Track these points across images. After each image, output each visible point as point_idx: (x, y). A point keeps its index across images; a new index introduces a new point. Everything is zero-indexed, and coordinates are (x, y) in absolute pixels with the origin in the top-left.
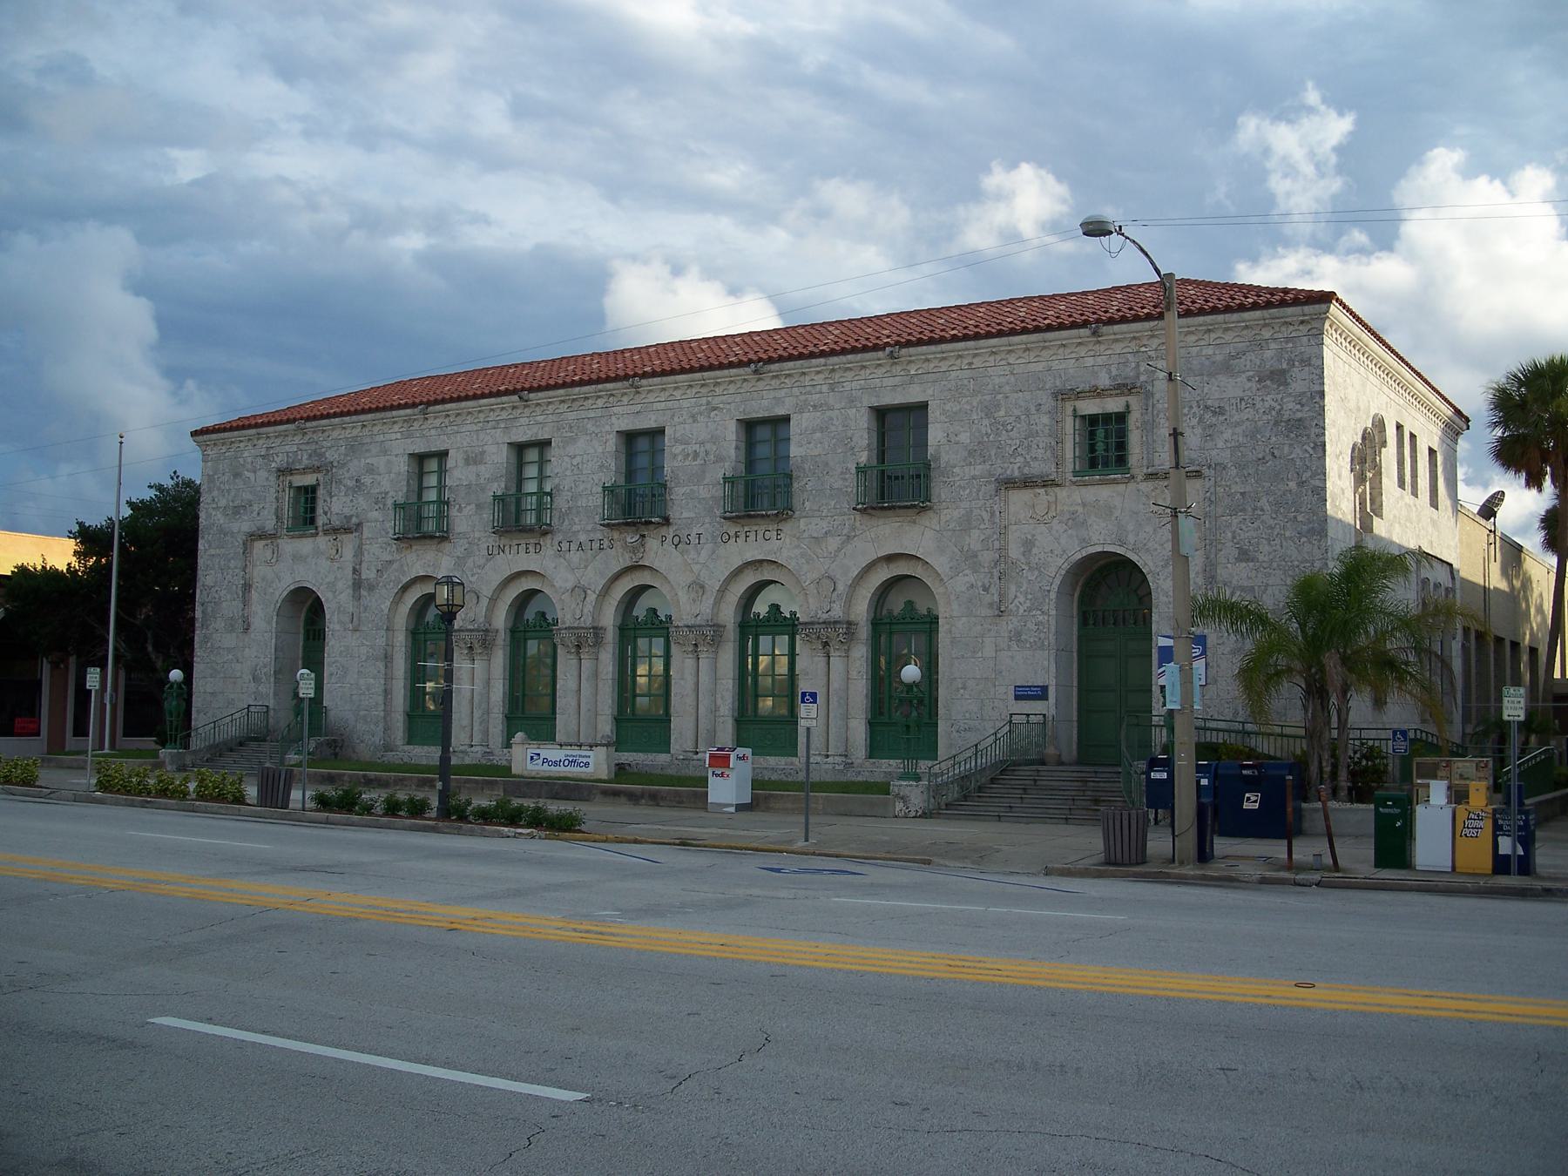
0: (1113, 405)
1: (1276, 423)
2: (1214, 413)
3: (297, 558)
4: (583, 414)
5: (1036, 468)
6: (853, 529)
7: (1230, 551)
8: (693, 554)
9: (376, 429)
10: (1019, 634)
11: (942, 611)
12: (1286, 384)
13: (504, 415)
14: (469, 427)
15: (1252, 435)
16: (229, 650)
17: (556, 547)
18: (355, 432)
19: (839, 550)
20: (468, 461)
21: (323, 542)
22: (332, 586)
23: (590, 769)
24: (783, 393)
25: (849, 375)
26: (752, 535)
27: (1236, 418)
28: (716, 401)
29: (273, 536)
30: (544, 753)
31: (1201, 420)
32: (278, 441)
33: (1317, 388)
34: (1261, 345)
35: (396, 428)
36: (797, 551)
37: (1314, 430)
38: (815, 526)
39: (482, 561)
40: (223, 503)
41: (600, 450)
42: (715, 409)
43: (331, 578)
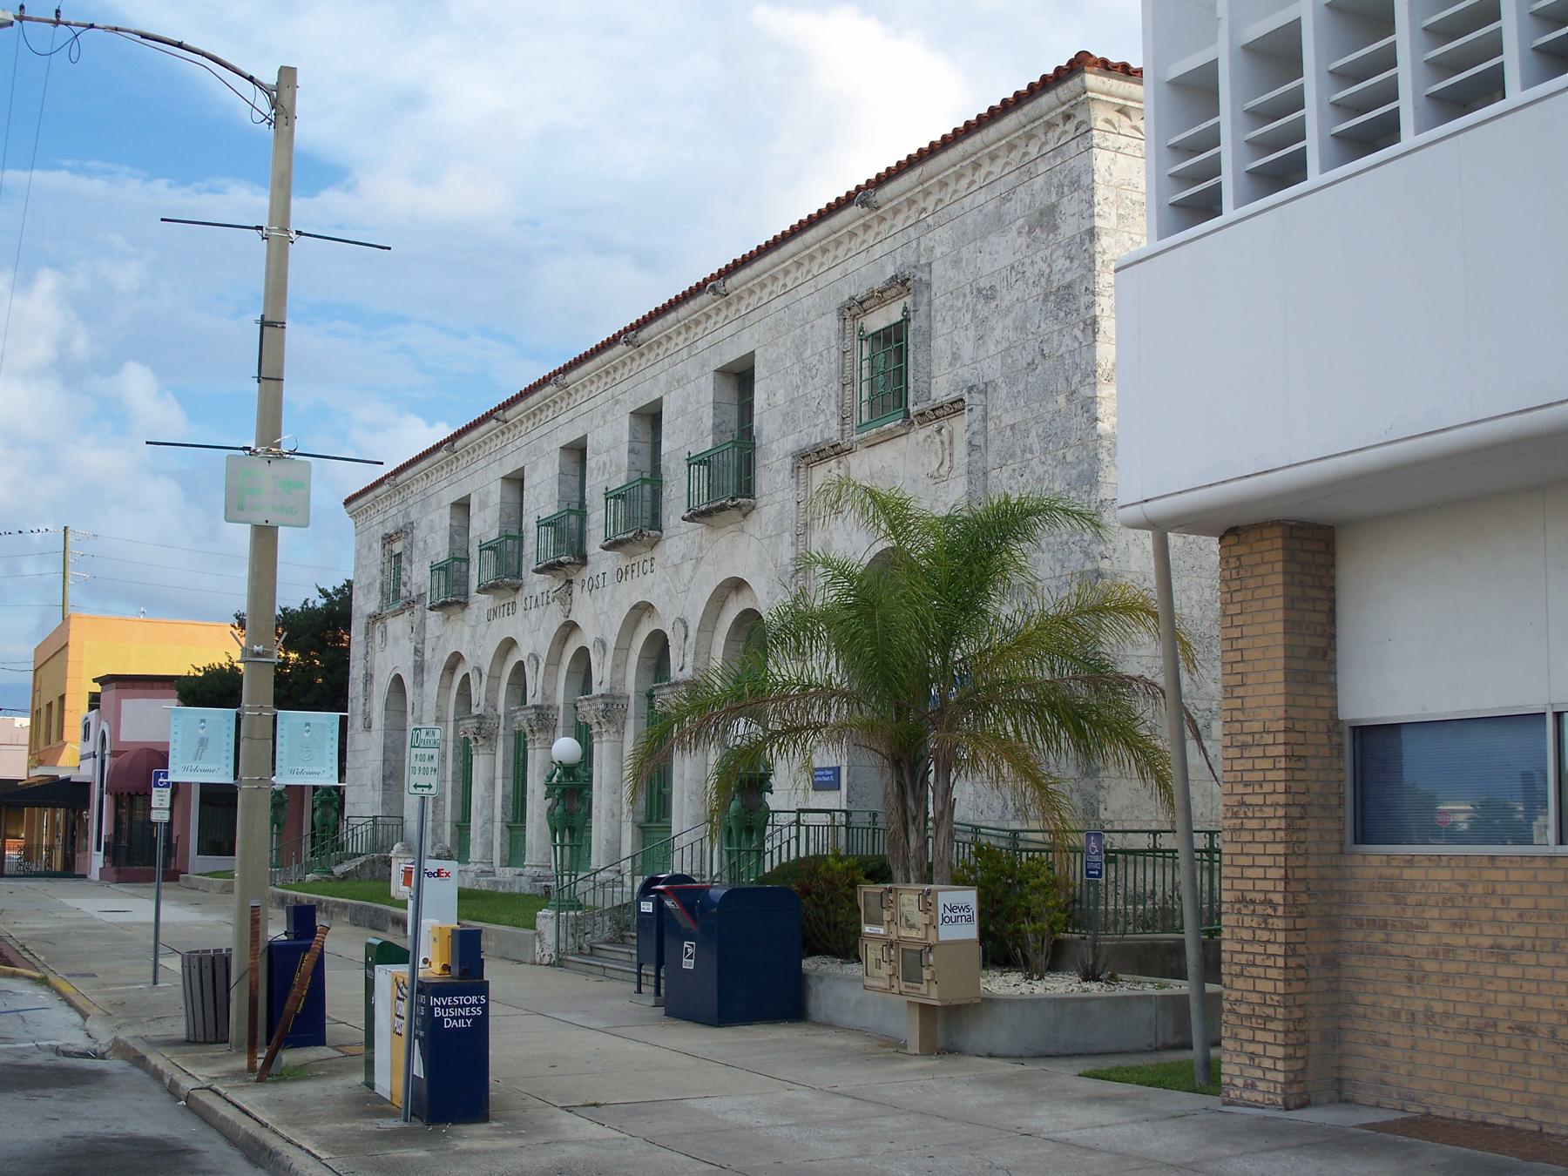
0: (893, 313)
2: (986, 297)
15: (1021, 328)
31: (974, 317)
33: (1087, 226)
37: (1084, 300)
42: (617, 402)
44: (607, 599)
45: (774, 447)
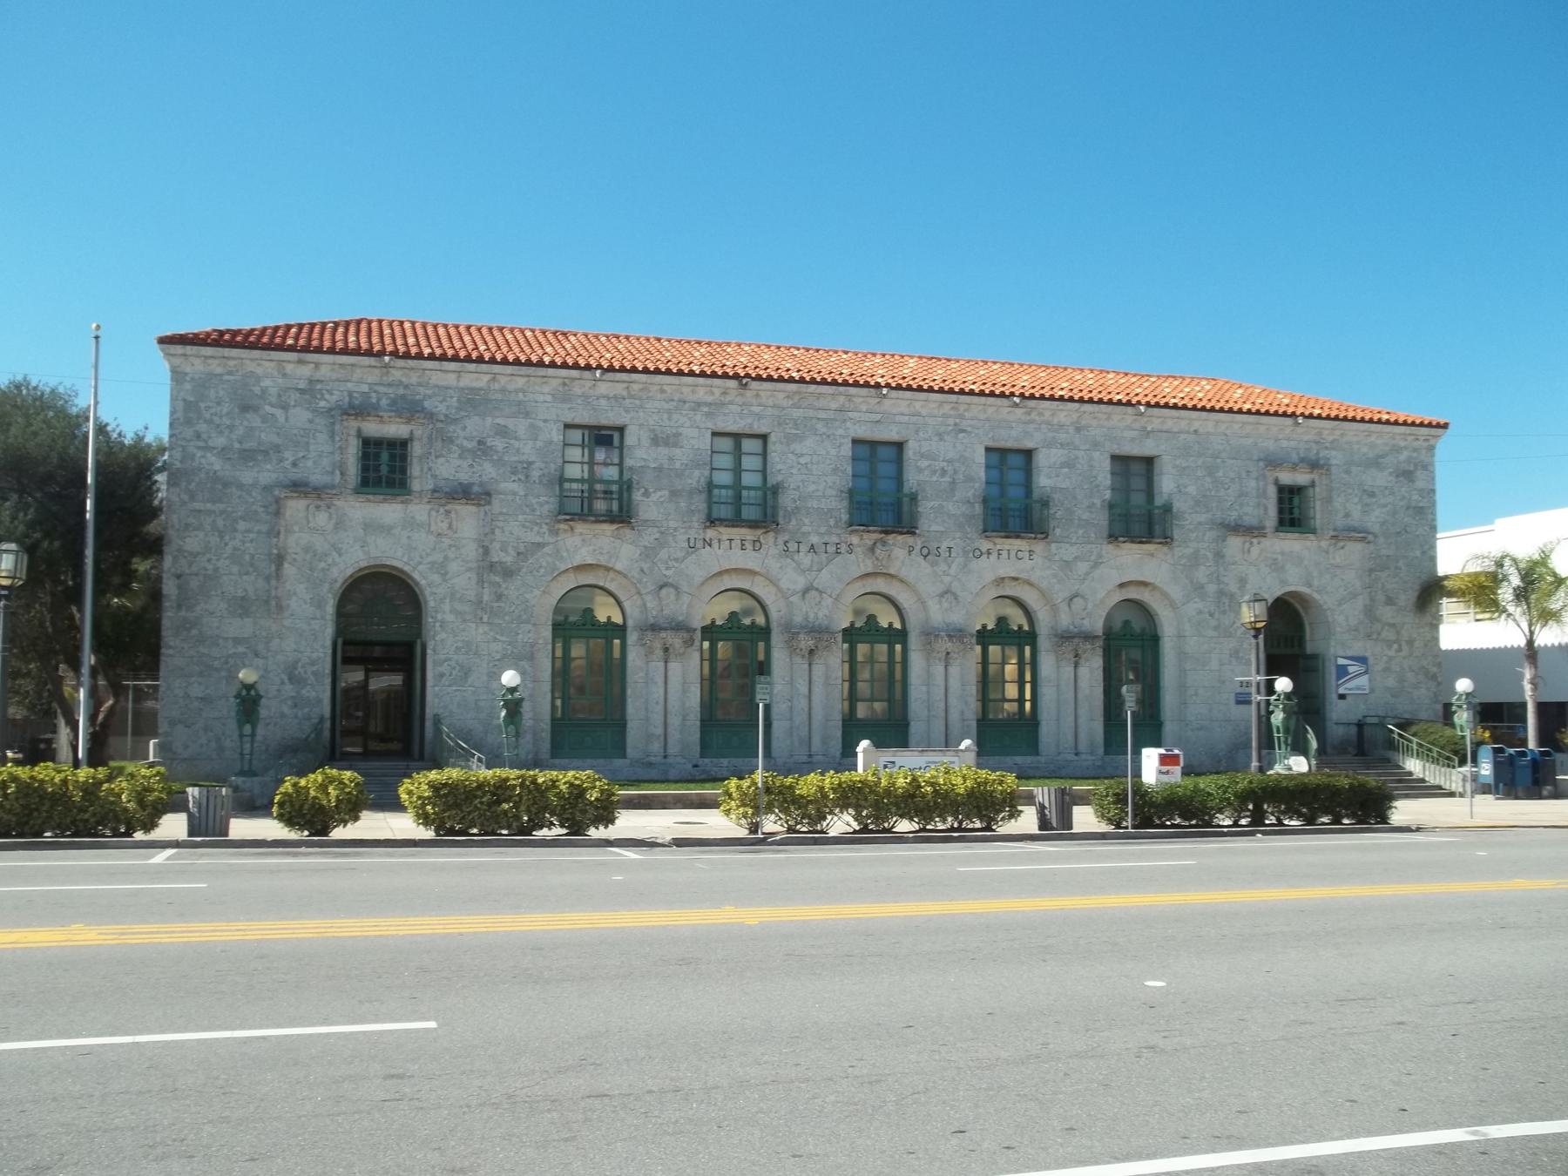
0: (1301, 478)
4: (811, 413)
5: (1249, 520)
6: (1100, 556)
7: (1381, 597)
8: (943, 567)
11: (1167, 630)
12: (1413, 481)
16: (237, 641)
17: (781, 547)
19: (1088, 574)
20: (656, 441)
21: (419, 510)
22: (441, 568)
26: (1005, 554)
36: (1048, 572)
38: (1067, 552)
39: (680, 554)
40: (220, 441)
41: (833, 452)
42: (963, 431)
43: (438, 557)
44: (954, 566)
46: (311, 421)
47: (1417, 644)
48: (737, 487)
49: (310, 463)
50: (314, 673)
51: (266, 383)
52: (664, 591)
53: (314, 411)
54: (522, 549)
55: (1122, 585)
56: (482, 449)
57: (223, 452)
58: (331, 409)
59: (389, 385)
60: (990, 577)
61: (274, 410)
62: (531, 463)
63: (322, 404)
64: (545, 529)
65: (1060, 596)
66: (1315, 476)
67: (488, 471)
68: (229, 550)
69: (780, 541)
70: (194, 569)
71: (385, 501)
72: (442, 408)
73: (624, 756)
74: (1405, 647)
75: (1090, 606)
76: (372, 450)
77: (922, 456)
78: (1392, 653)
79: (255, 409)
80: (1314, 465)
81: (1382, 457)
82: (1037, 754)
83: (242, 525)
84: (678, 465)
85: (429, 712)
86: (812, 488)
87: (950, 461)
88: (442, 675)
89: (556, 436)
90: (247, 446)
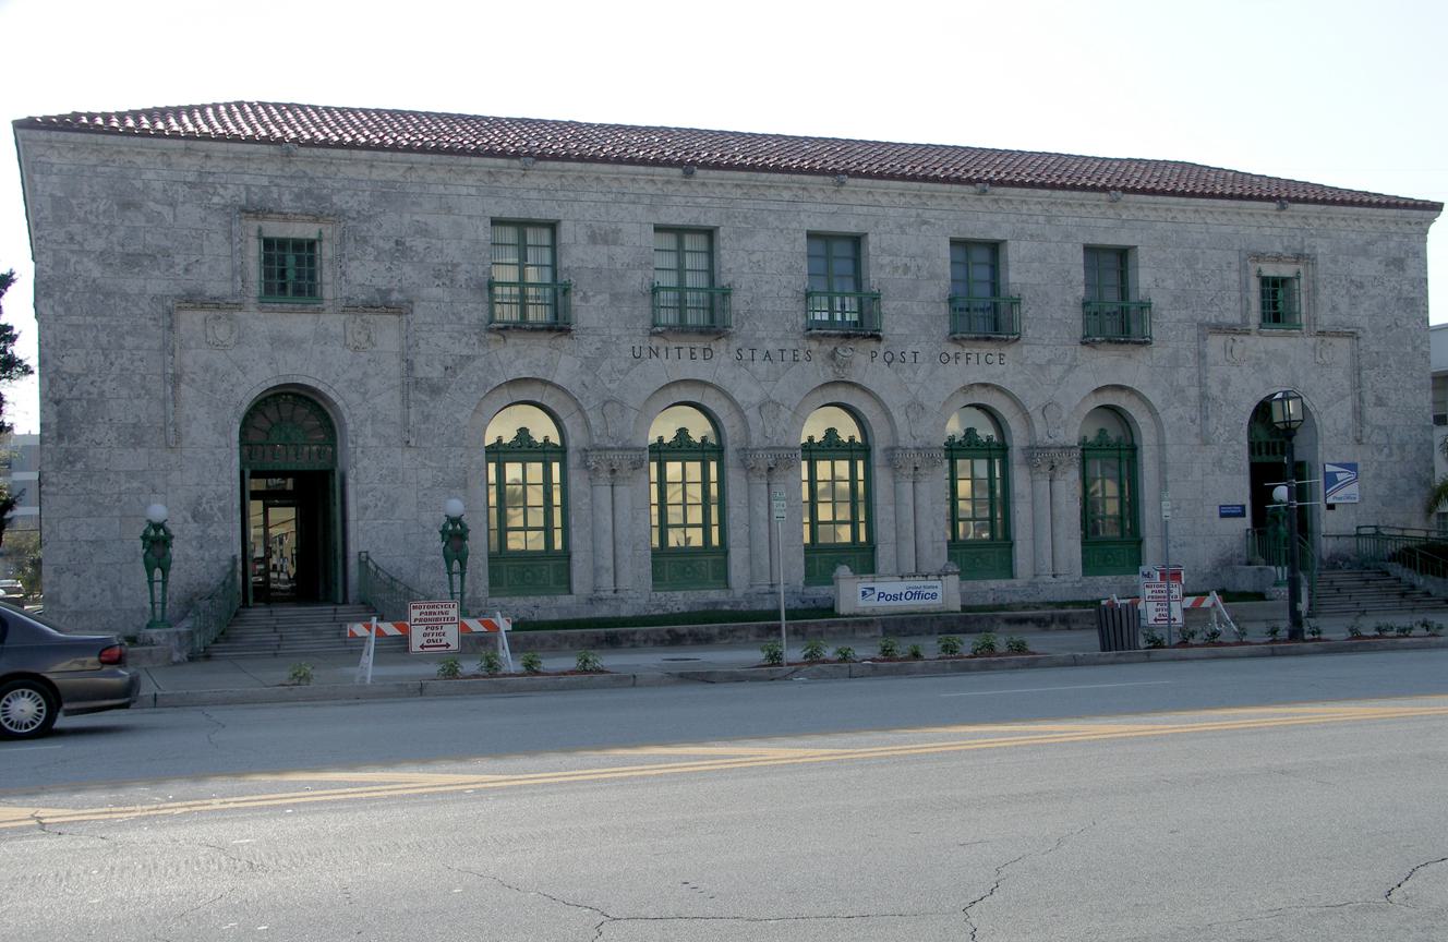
0: (1285, 271)
1: (1398, 299)
3: (281, 342)
9: (431, 177)
10: (1220, 460)
12: (1403, 270)
13: (650, 189)
14: (594, 196)
16: (131, 475)
17: (734, 354)
18: (391, 175)
20: (594, 238)
21: (333, 322)
23: (939, 600)
24: (999, 218)
25: (1066, 210)
26: (973, 358)
27: (1372, 292)
28: (927, 215)
29: (239, 306)
30: (880, 587)
31: (1348, 291)
32: (229, 166)
34: (1387, 236)
35: (470, 180)
39: (624, 365)
40: (99, 244)
41: (787, 248)
44: (921, 373)
45: (1164, 313)
46: (203, 220)
47: (1408, 448)
48: (681, 288)
49: (205, 269)
50: (220, 509)
51: (150, 175)
52: (608, 408)
53: (206, 208)
54: (449, 363)
55: (1098, 390)
56: (401, 248)
57: (103, 257)
58: (225, 206)
59: (292, 177)
60: (959, 384)
61: (159, 208)
62: (456, 265)
63: (216, 200)
64: (475, 339)
65: (1033, 404)
66: (1301, 268)
67: (409, 273)
68: (115, 370)
69: (733, 348)
70: (75, 392)
71: (293, 311)
72: (353, 203)
73: (571, 593)
74: (1395, 451)
75: (1065, 416)
76: (275, 252)
77: (883, 251)
78: (1382, 458)
79: (138, 207)
80: (1299, 257)
81: (1369, 243)
82: (1012, 576)
83: (129, 341)
84: (618, 266)
85: (353, 550)
86: (766, 288)
87: (913, 257)
88: (366, 508)
89: (484, 233)
90: (131, 250)
